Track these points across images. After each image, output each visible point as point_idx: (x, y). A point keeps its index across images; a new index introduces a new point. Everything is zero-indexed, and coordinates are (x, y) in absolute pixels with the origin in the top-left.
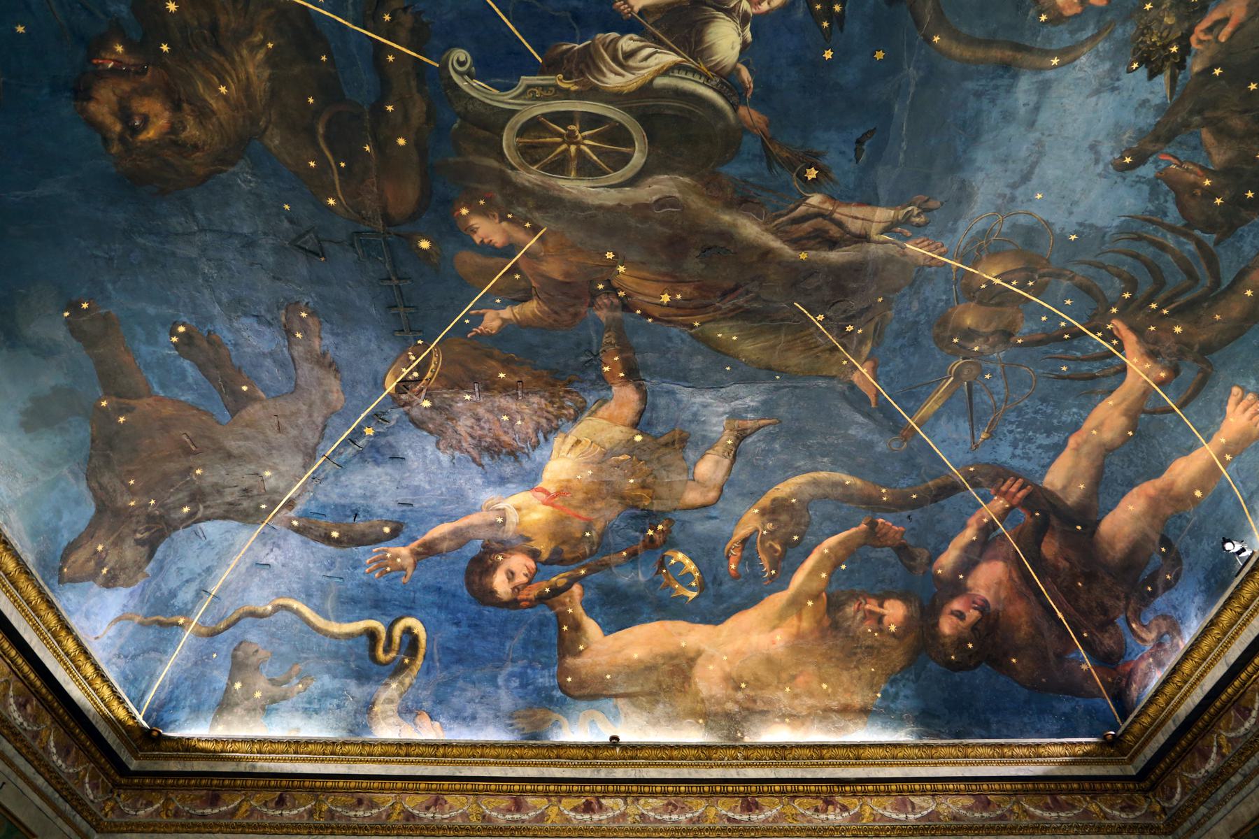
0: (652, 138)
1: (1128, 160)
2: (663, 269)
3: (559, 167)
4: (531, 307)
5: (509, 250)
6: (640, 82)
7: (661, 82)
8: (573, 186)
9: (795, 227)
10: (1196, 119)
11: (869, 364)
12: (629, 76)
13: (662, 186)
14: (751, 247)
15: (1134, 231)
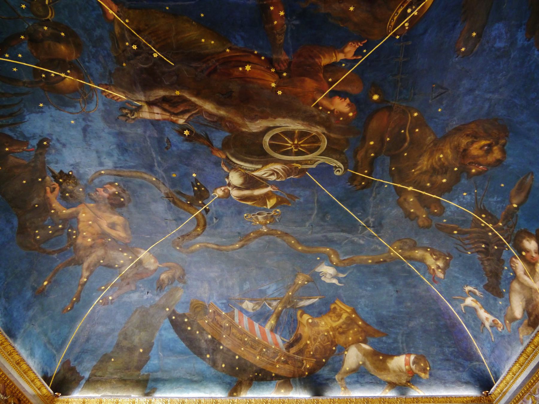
0: (261, 145)
1: (45, 143)
2: (251, 85)
3: (302, 134)
4: (325, 61)
5: (334, 94)
6: (268, 166)
7: (259, 167)
8: (297, 126)
9: (187, 108)
10: (33, 164)
11: (112, 18)
12: (272, 168)
13: (255, 127)
14: (207, 98)
15: (17, 119)
